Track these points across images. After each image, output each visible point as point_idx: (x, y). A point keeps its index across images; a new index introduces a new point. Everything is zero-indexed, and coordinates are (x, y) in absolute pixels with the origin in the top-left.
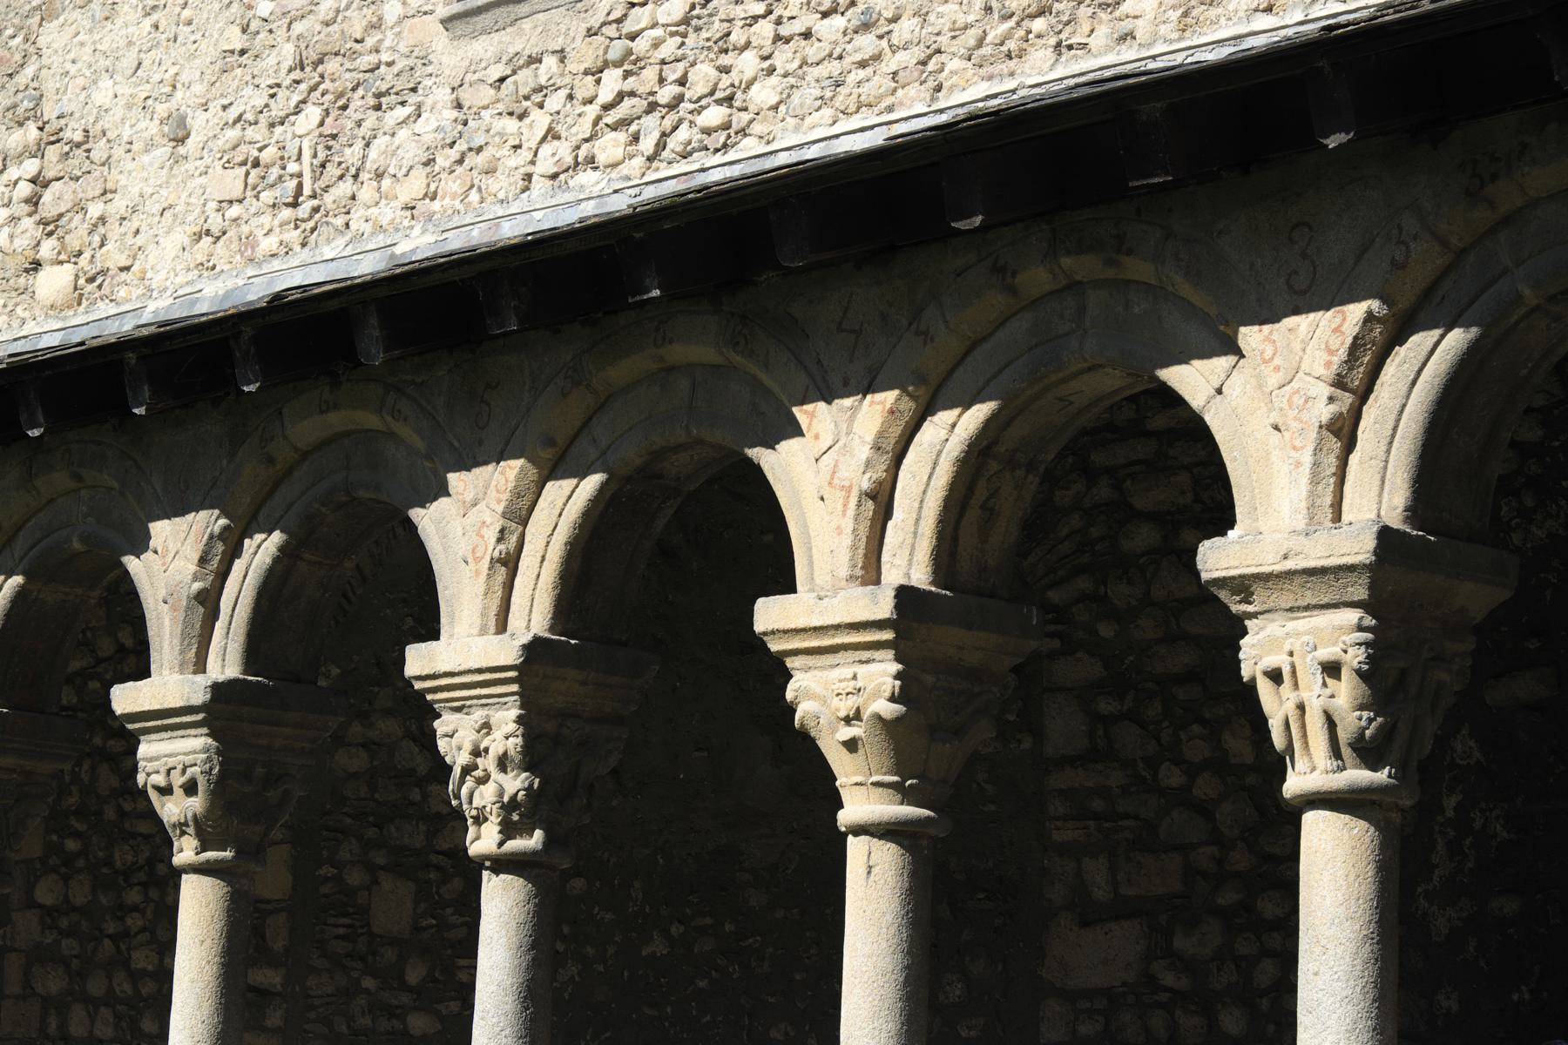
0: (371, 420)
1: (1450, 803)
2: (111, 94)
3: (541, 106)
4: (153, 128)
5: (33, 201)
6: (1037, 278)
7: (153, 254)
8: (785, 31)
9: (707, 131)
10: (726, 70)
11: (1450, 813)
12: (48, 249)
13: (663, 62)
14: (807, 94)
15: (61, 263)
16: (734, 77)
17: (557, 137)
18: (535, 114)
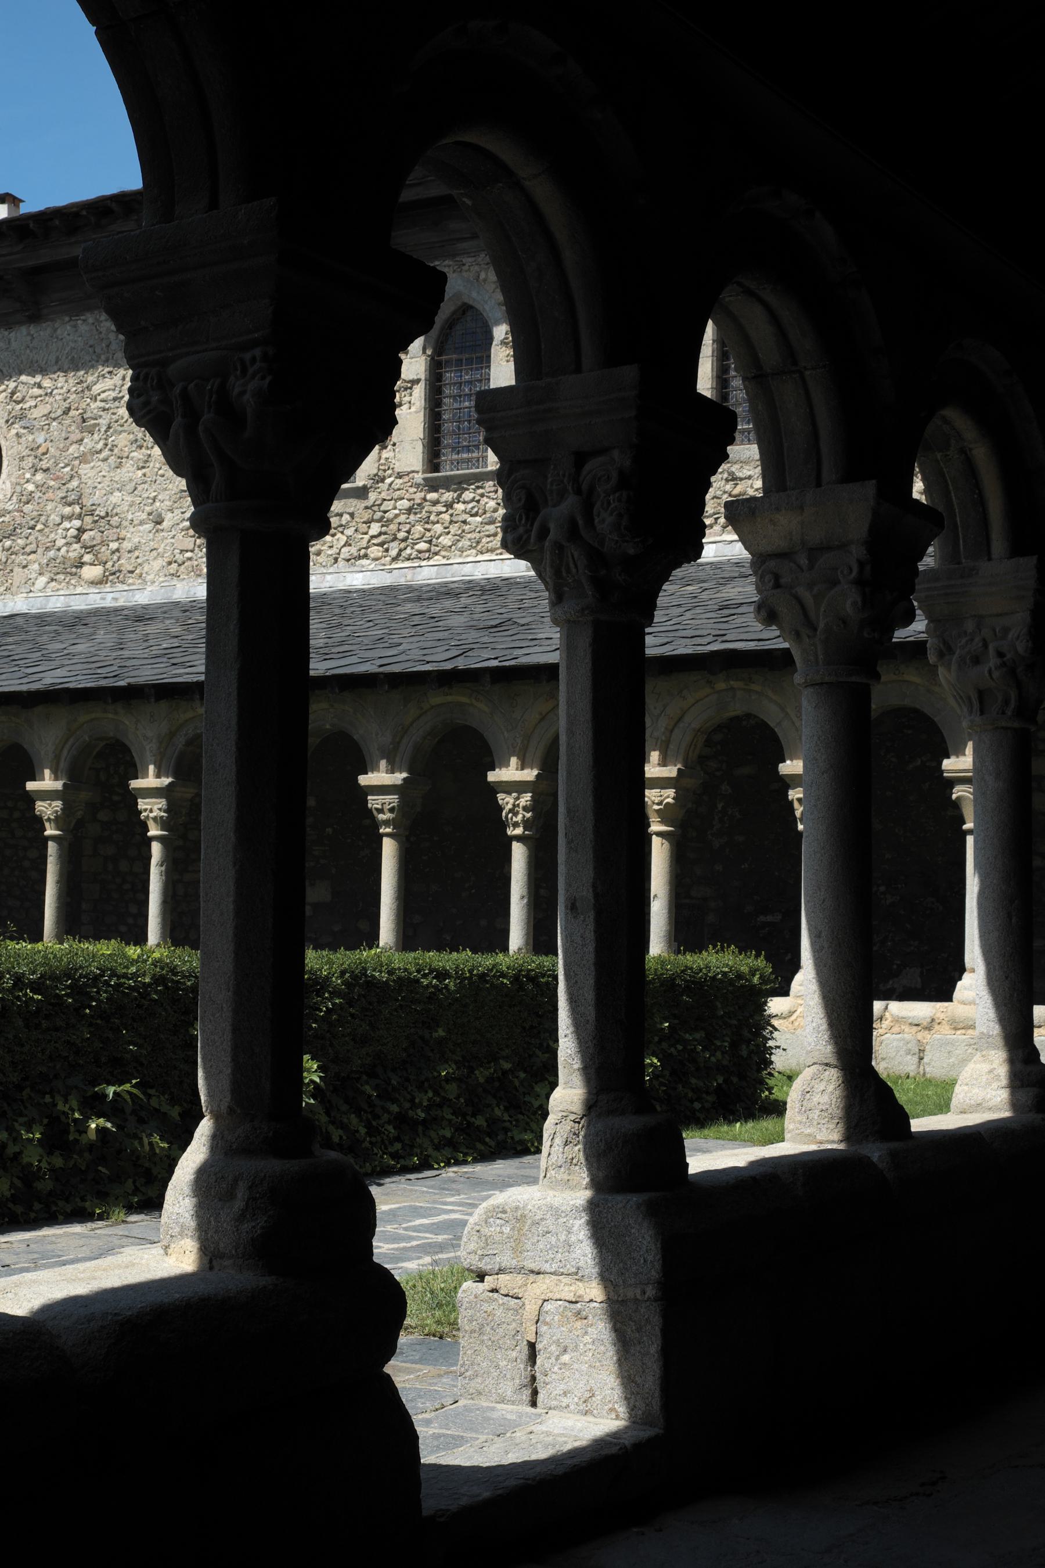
0: (464, 700)
1: (720, 806)
2: (120, 499)
3: (342, 533)
4: (144, 516)
5: (78, 539)
6: (721, 685)
7: (146, 568)
8: (455, 519)
9: (420, 552)
10: (429, 530)
11: (720, 809)
12: (87, 558)
13: (400, 524)
14: (465, 543)
15: (95, 565)
16: (432, 533)
17: (350, 545)
18: (339, 535)
